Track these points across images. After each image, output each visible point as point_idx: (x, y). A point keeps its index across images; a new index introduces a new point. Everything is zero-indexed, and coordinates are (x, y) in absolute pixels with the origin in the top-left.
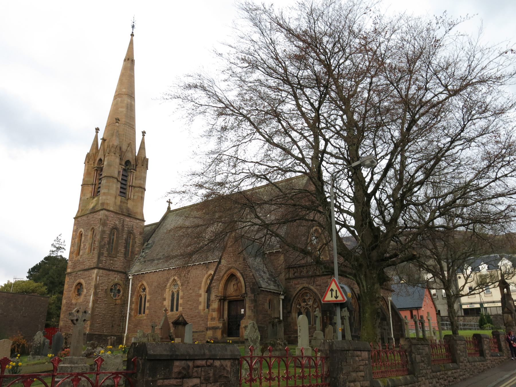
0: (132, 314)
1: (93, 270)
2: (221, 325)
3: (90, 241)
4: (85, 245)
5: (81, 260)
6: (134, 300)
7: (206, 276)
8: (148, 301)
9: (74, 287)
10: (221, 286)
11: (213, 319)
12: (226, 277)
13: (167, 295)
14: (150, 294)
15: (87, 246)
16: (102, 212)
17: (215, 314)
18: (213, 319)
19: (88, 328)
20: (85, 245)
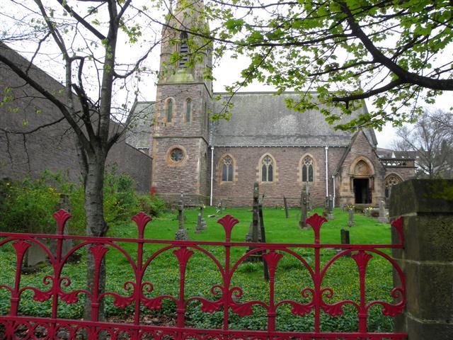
0: (217, 180)
1: (197, 139)
2: (353, 195)
3: (185, 111)
4: (178, 114)
5: (176, 126)
6: (217, 168)
7: (303, 157)
8: (236, 171)
9: (168, 151)
10: (352, 168)
11: (345, 190)
12: (356, 162)
13: (260, 167)
14: (237, 165)
15: (183, 114)
16: (199, 86)
17: (348, 187)
18: (345, 190)
19: (198, 190)
20: (178, 114)
